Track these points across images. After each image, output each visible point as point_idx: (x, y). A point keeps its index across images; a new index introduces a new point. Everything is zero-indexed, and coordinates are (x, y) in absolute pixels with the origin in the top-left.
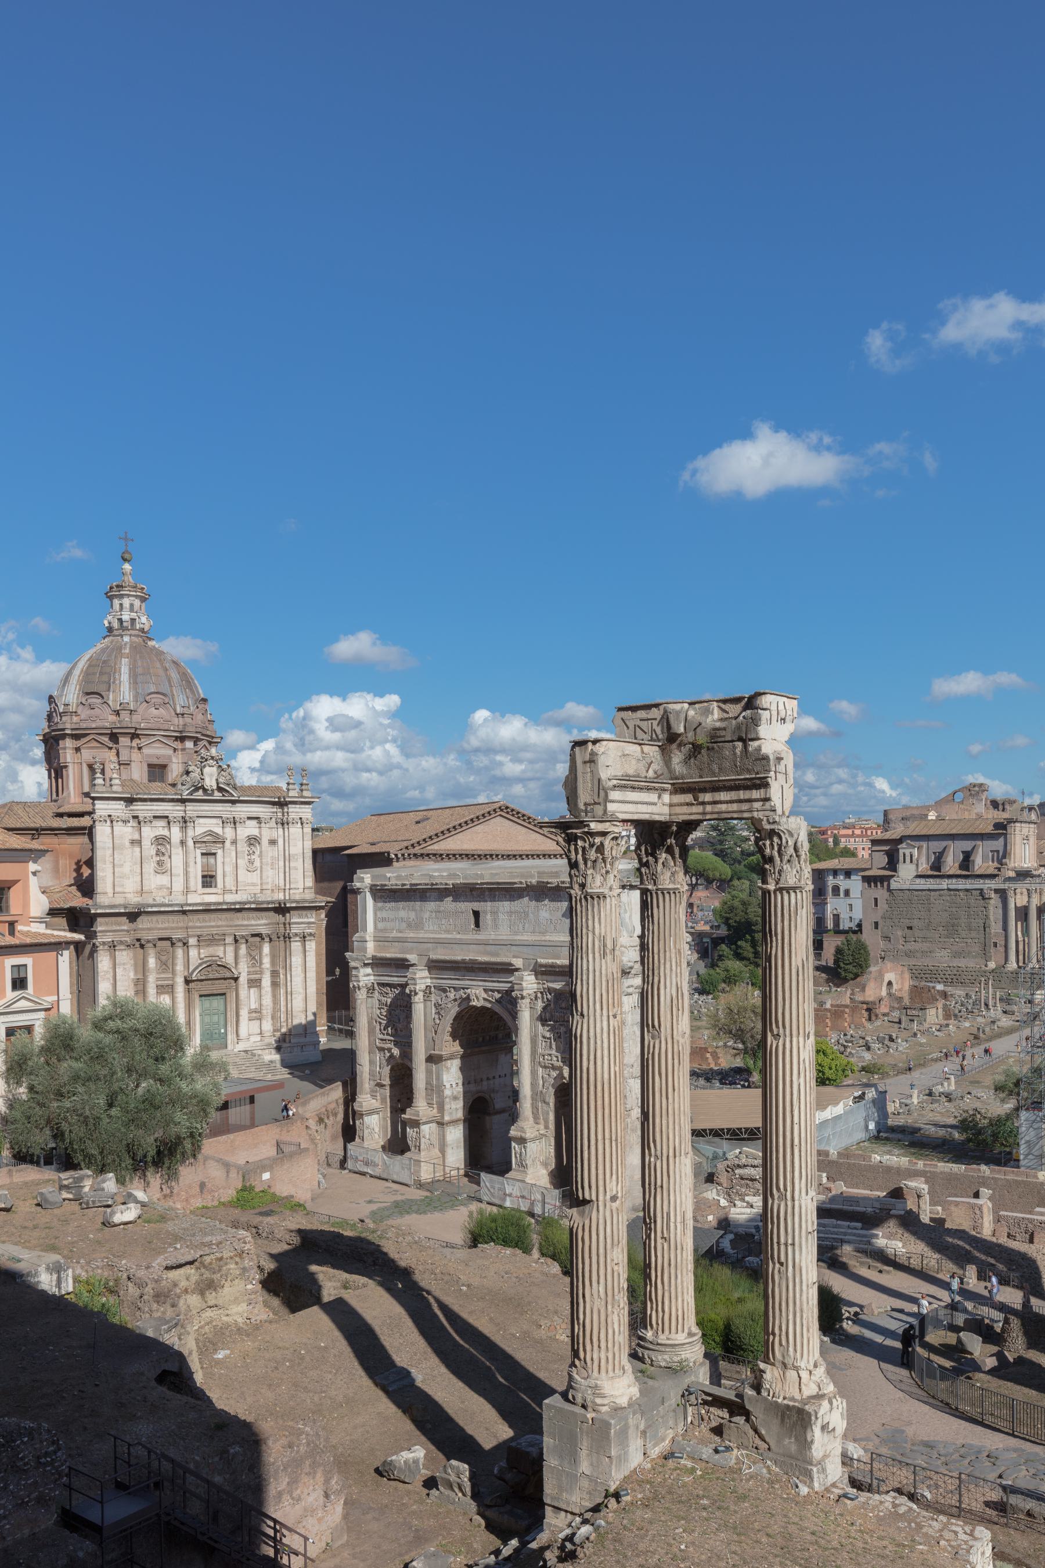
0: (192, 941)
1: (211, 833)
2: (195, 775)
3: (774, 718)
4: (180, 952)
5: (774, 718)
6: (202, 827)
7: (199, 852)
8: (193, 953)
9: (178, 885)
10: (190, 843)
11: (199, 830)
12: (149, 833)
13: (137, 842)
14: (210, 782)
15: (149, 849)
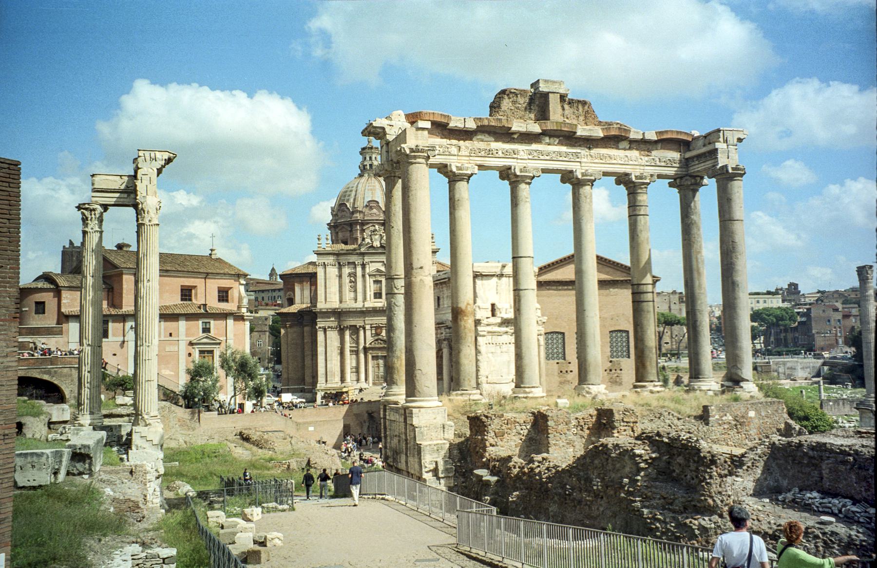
0: (368, 327)
1: (378, 270)
2: (368, 240)
3: (148, 158)
4: (362, 333)
5: (148, 158)
6: (371, 268)
7: (372, 280)
8: (368, 333)
9: (360, 297)
10: (367, 276)
11: (372, 269)
12: (346, 270)
13: (340, 276)
14: (377, 244)
15: (346, 280)
